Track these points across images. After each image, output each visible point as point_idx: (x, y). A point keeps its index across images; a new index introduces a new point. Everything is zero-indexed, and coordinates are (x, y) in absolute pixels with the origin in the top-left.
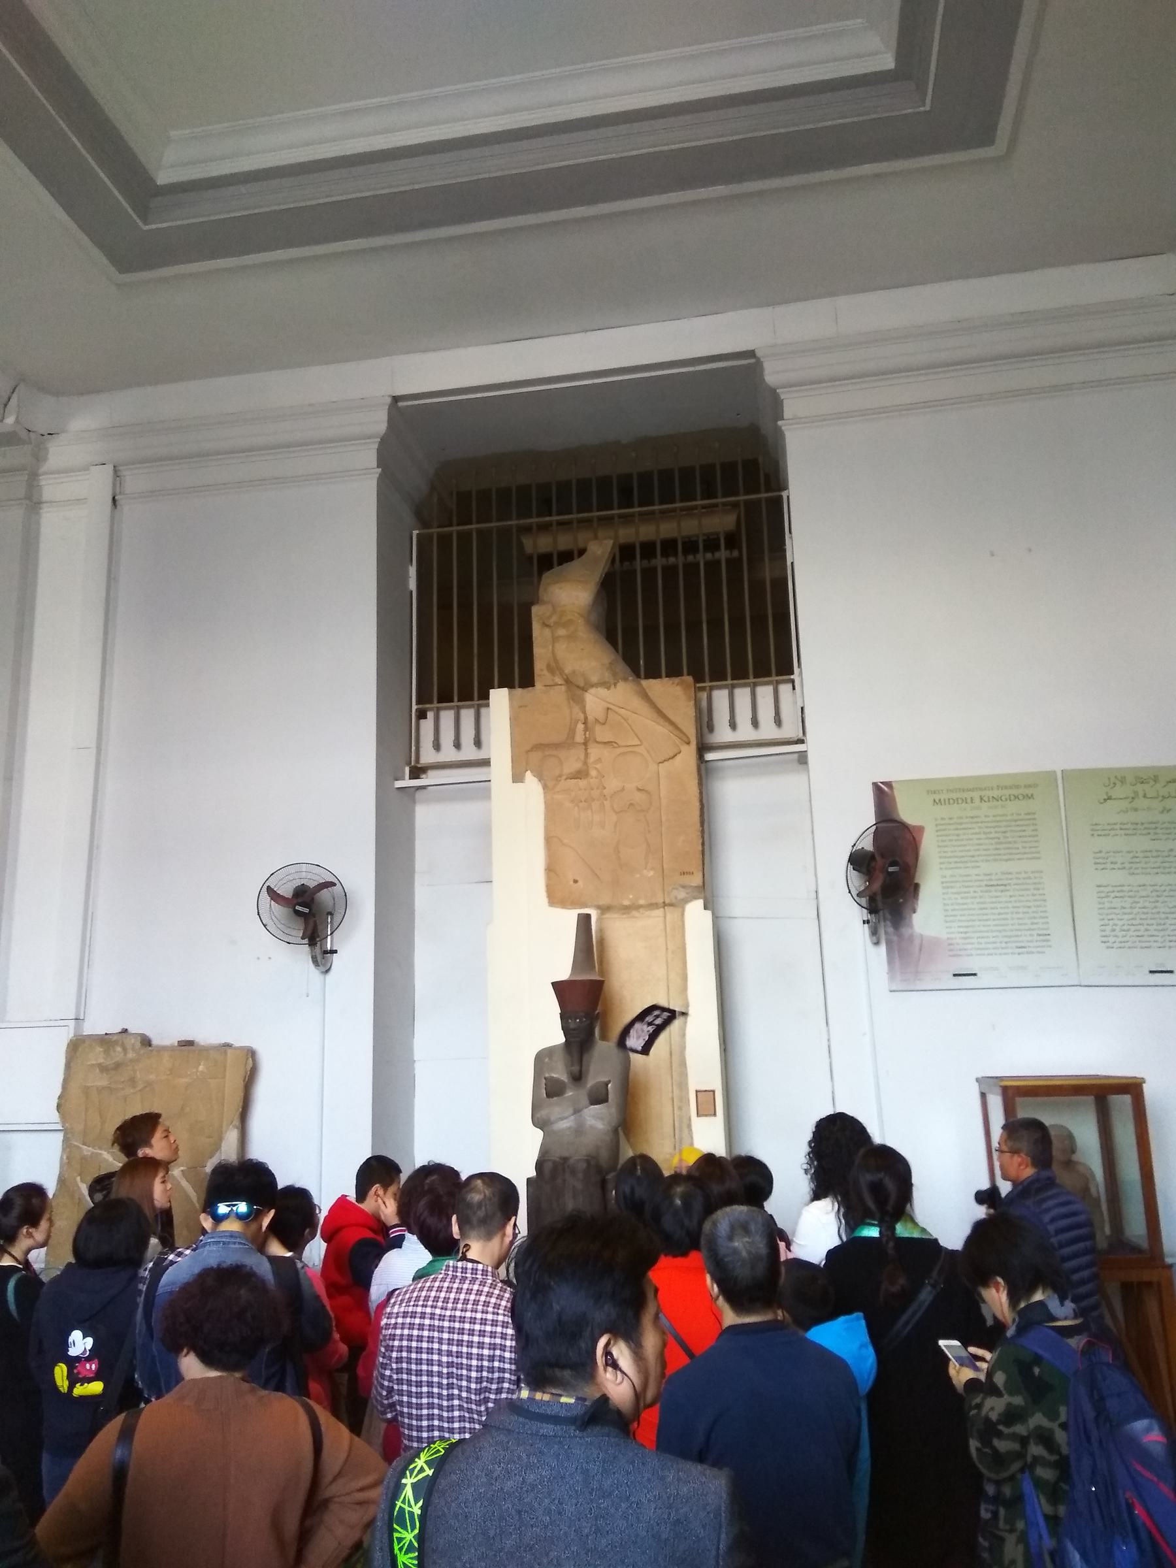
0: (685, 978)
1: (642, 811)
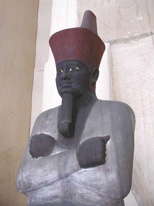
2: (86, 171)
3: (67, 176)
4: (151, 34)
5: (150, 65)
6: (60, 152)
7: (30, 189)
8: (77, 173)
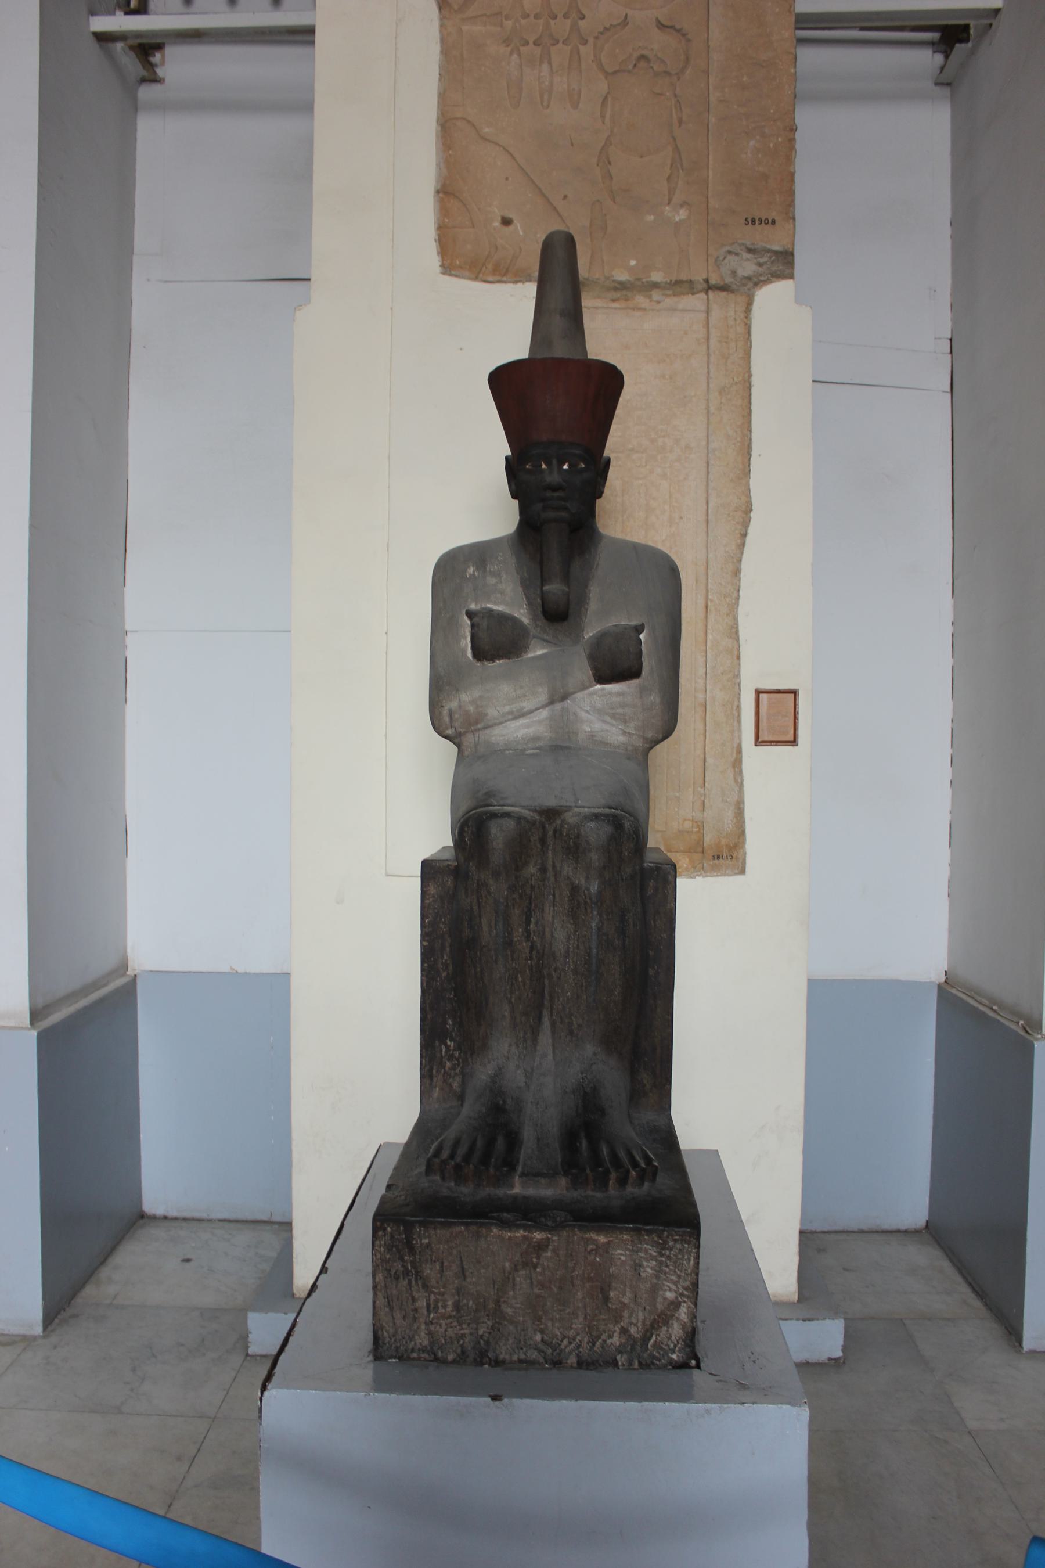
1: (667, 73)
2: (604, 689)
3: (564, 698)
4: (705, 285)
7: (479, 726)
8: (586, 692)
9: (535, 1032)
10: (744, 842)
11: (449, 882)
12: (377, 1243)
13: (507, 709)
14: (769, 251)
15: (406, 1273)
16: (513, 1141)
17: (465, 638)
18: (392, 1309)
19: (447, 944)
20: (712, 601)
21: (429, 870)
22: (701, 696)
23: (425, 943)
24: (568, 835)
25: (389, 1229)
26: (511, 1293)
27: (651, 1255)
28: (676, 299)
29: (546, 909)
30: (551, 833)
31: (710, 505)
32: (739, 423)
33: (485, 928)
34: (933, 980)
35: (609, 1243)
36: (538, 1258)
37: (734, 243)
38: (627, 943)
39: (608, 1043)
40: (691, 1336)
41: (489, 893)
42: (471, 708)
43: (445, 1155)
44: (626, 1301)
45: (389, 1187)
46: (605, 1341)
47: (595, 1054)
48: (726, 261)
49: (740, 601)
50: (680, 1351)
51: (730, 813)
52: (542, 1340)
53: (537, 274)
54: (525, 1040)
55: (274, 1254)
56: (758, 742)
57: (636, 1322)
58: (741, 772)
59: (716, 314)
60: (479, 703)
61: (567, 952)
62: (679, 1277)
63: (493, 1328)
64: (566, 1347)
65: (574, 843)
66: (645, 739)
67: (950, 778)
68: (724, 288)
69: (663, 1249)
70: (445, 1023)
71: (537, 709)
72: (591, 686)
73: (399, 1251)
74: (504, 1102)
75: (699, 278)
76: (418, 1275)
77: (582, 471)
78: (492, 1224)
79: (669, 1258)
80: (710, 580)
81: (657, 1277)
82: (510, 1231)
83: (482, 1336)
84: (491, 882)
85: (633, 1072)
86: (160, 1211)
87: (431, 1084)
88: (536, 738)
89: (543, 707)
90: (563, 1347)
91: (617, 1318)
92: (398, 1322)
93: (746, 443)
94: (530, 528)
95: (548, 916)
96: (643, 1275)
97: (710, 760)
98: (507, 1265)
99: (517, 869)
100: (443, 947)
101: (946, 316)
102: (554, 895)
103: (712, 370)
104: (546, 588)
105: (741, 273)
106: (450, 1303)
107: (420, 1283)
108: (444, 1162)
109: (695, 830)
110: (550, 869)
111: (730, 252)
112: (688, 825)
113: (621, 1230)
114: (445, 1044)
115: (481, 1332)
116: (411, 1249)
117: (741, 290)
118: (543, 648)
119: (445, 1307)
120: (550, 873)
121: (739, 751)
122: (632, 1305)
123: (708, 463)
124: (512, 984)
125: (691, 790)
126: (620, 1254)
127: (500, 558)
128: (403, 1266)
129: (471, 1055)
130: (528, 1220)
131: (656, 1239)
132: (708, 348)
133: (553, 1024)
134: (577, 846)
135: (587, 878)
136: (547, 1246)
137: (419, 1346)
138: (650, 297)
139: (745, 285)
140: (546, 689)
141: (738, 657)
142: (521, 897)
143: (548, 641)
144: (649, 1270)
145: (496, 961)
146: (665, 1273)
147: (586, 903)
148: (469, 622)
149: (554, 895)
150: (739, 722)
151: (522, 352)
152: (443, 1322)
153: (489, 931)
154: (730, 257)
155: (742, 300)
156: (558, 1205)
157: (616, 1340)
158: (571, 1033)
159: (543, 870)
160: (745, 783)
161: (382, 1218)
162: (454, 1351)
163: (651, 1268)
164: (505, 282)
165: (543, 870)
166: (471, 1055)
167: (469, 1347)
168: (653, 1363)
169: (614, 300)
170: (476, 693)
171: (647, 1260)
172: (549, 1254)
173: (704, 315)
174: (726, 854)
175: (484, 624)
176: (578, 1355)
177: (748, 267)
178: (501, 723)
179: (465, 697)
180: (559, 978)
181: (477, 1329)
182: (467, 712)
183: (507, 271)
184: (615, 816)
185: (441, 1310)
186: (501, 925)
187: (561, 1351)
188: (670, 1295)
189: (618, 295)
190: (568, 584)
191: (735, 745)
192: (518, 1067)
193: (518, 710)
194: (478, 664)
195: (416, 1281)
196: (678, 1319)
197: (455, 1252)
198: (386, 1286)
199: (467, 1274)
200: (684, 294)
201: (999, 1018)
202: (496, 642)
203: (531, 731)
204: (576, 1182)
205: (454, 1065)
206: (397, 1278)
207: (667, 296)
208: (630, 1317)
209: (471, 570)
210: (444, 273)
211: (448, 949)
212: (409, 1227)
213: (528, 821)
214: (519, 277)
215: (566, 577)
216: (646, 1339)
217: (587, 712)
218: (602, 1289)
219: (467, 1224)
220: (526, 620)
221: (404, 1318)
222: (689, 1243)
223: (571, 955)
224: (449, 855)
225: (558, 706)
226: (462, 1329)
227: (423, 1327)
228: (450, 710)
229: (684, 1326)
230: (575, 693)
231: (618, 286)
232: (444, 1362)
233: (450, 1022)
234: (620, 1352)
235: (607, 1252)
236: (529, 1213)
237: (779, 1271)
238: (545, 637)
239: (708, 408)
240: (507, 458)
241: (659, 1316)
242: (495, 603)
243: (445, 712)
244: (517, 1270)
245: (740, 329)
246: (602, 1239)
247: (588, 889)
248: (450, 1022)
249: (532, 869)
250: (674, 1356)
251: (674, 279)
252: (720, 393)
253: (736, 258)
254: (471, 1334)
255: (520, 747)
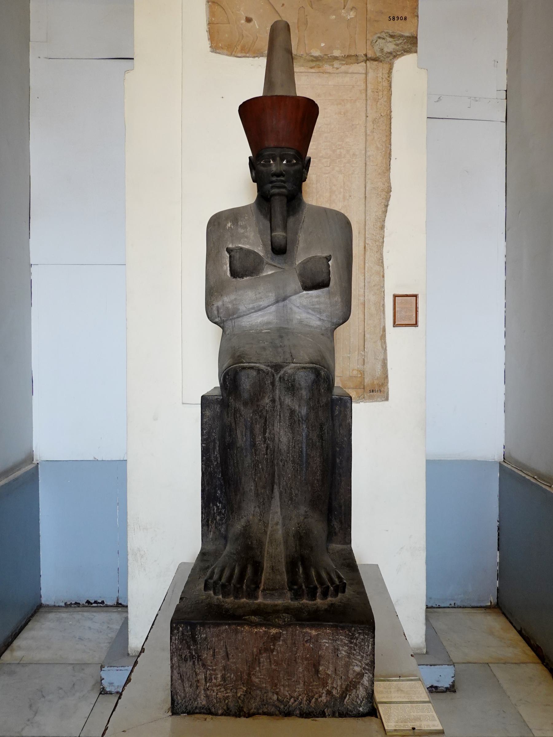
0: (388, 155)
3: (284, 299)
4: (365, 58)
5: (353, 125)
6: (273, 272)
8: (298, 295)
9: (271, 497)
10: (387, 383)
11: (218, 408)
12: (173, 638)
13: (251, 306)
14: (402, 36)
15: (192, 657)
16: (258, 568)
17: (226, 264)
18: (183, 681)
19: (217, 445)
20: (368, 244)
21: (206, 401)
22: (362, 298)
23: (203, 445)
24: (288, 380)
25: (181, 629)
26: (258, 669)
27: (345, 643)
28: (348, 66)
29: (276, 425)
30: (277, 379)
31: (367, 188)
32: (384, 140)
33: (239, 436)
34: (496, 460)
35: (318, 635)
36: (274, 645)
37: (382, 32)
38: (324, 444)
39: (314, 504)
40: (371, 696)
41: (241, 415)
42: (230, 306)
43: (216, 577)
44: (329, 672)
45: (181, 599)
46: (317, 699)
47: (306, 512)
48: (377, 43)
49: (384, 244)
50: (364, 706)
51: (379, 367)
52: (278, 699)
53: (266, 52)
54: (264, 504)
55: (119, 627)
56: (395, 325)
57: (337, 685)
58: (385, 342)
59: (371, 75)
60: (234, 302)
61: (288, 450)
62: (362, 657)
63: (246, 691)
64: (293, 703)
65: (292, 385)
66: (333, 323)
67: (504, 344)
68: (375, 59)
69: (352, 639)
70: (216, 492)
71: (269, 306)
72: (300, 292)
73: (187, 642)
74: (252, 543)
75: (361, 53)
76: (199, 658)
77: (295, 164)
78: (245, 624)
79: (356, 644)
80: (367, 233)
81: (349, 657)
82: (256, 628)
83: (239, 697)
84: (242, 408)
85: (329, 521)
86: (51, 603)
87: (208, 530)
88: (268, 323)
89: (272, 305)
90: (290, 703)
91: (325, 684)
92: (187, 689)
93: (388, 152)
94: (264, 199)
95: (276, 428)
96: (340, 656)
97: (367, 336)
98: (255, 650)
99: (258, 400)
100: (214, 448)
101: (505, 76)
102: (280, 416)
103: (369, 109)
104: (273, 234)
105: (386, 50)
106: (219, 676)
107: (200, 663)
108: (215, 583)
109: (359, 375)
110: (277, 399)
111: (379, 38)
112: (355, 372)
113: (325, 627)
114: (216, 505)
115: (239, 695)
116: (195, 641)
117: (386, 59)
118: (271, 270)
119: (216, 678)
120: (277, 403)
121: (384, 330)
122: (333, 676)
123: (366, 164)
124: (256, 469)
125: (357, 352)
126: (326, 643)
127: (246, 218)
128: (190, 652)
129: (232, 513)
130: (267, 621)
131: (347, 632)
132: (366, 95)
133: (281, 494)
134: (293, 386)
135: (299, 406)
136: (280, 637)
137: (200, 705)
138: (333, 65)
139: (388, 57)
140: (274, 294)
141: (383, 277)
142: (260, 417)
143: (275, 266)
144: (343, 652)
145: (246, 456)
146: (354, 655)
147: (299, 420)
148: (228, 256)
149: (280, 416)
150: (384, 313)
151: (257, 91)
152: (215, 688)
153: (242, 439)
154: (379, 41)
155: (386, 66)
156: (287, 609)
157: (324, 699)
158: (291, 499)
159: (273, 401)
160: (388, 348)
161: (175, 623)
162: (222, 708)
163: (345, 651)
164: (248, 57)
165: (273, 401)
166: (232, 513)
167: (231, 705)
168: (348, 714)
169: (311, 68)
170: (232, 297)
171: (342, 646)
172: (281, 643)
173: (364, 76)
174: (378, 390)
175: (237, 256)
176: (300, 709)
177: (390, 47)
178: (247, 315)
179: (226, 299)
180: (284, 466)
181: (236, 692)
182: (227, 308)
183: (249, 50)
184: (315, 369)
185: (214, 681)
186: (248, 433)
187: (289, 706)
188: (357, 669)
189: (314, 64)
190: (286, 232)
191: (382, 327)
192: (260, 520)
193: (258, 307)
194: (234, 280)
195: (198, 661)
196: (362, 684)
197: (222, 642)
198: (179, 666)
199: (230, 657)
200: (352, 63)
201: (538, 483)
202: (243, 267)
203: (265, 319)
204: (297, 595)
205: (222, 518)
206: (186, 660)
207: (343, 64)
208: (332, 683)
209: (229, 225)
210: (212, 52)
211: (217, 448)
212: (193, 627)
213: (264, 372)
214: (257, 54)
215: (285, 228)
216: (343, 697)
217: (298, 307)
218: (314, 665)
219: (229, 625)
220: (261, 254)
221: (191, 686)
222: (368, 635)
223: (291, 452)
224: (218, 392)
225: (281, 304)
226: (227, 693)
227: (203, 692)
228: (218, 307)
229: (366, 689)
230: (290, 296)
231: (314, 59)
232: (216, 715)
233: (219, 492)
234: (327, 707)
235: (317, 641)
236: (266, 616)
237: (415, 631)
238: (273, 263)
239: (366, 131)
240: (250, 158)
241: (350, 682)
242: (243, 244)
243: (214, 308)
244: (261, 653)
245: (385, 84)
246: (314, 633)
247: (300, 412)
248: (219, 492)
249: (267, 400)
250: (361, 709)
251: (347, 54)
252: (373, 123)
253: (383, 41)
254: (233, 696)
255: (259, 329)
